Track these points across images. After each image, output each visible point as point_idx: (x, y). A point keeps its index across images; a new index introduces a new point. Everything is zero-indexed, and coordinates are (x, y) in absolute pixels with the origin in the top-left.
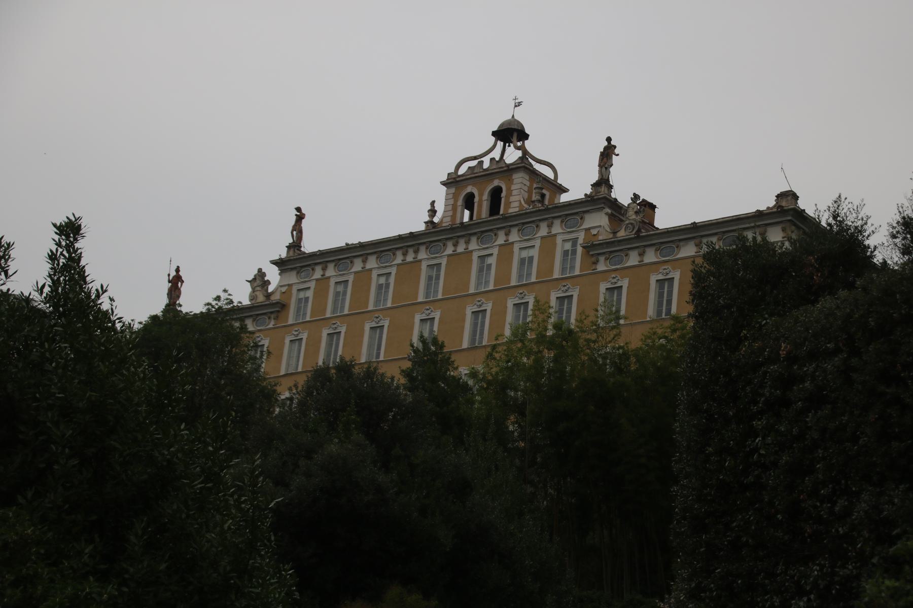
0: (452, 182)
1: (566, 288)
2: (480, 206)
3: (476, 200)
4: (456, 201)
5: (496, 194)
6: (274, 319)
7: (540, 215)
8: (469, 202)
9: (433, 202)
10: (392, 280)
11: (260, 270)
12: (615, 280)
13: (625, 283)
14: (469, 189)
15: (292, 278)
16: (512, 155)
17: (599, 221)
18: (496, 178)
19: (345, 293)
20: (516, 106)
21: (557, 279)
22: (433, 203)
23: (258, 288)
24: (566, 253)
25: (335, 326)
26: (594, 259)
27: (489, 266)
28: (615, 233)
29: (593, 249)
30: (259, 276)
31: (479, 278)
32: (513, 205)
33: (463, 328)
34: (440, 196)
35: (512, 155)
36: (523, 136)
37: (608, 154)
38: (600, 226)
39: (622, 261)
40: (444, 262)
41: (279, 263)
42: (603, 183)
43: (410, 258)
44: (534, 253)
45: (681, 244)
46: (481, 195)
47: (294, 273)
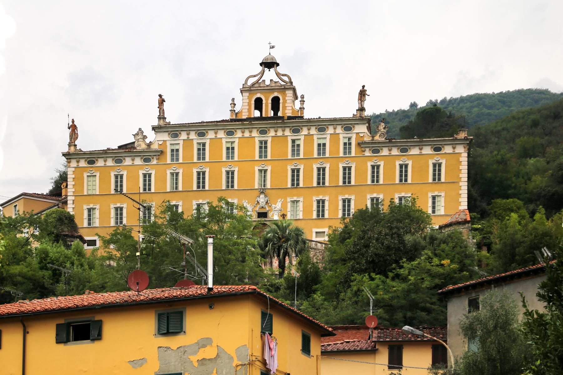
1: (348, 162)
2: (267, 106)
3: (264, 102)
4: (250, 101)
6: (157, 159)
7: (331, 122)
9: (233, 99)
11: (140, 129)
12: (376, 162)
14: (259, 95)
15: (165, 137)
17: (362, 129)
18: (276, 92)
19: (204, 150)
20: (271, 48)
21: (342, 157)
22: (233, 99)
23: (141, 140)
24: (345, 144)
25: (202, 167)
26: (363, 149)
27: (298, 146)
28: (373, 137)
29: (361, 145)
30: (141, 133)
31: (293, 151)
32: (288, 108)
33: (287, 176)
35: (270, 75)
38: (365, 132)
39: (379, 152)
41: (154, 128)
45: (411, 147)
46: (267, 100)
47: (167, 134)
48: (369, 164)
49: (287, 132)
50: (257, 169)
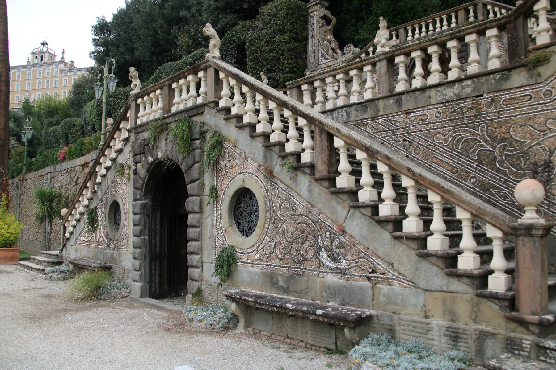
0: (33, 53)
5: (42, 57)
8: (36, 58)
10: (21, 74)
13: (67, 78)
14: (36, 55)
16: (45, 49)
17: (62, 66)
29: (61, 71)
34: (30, 56)
36: (47, 44)
37: (63, 52)
40: (31, 71)
42: (63, 58)
43: (24, 70)
44: (50, 71)
48: (63, 78)
49: (37, 68)
50: (27, 82)
